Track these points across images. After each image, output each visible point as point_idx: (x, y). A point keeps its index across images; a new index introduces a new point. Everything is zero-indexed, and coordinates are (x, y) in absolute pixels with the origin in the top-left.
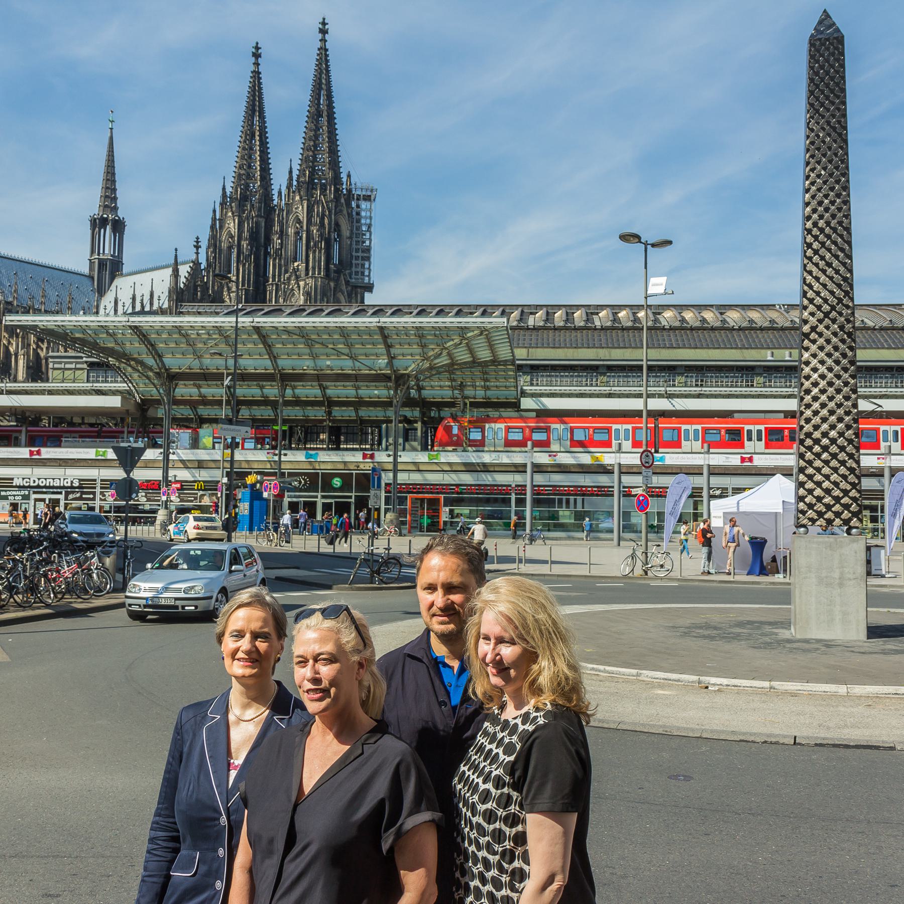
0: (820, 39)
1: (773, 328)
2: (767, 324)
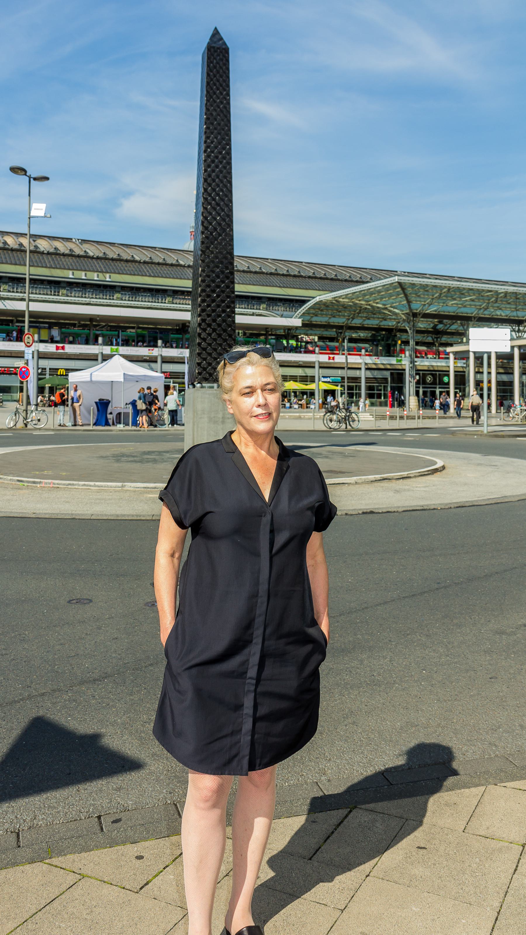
0: (214, 47)
1: (71, 255)
2: (67, 252)
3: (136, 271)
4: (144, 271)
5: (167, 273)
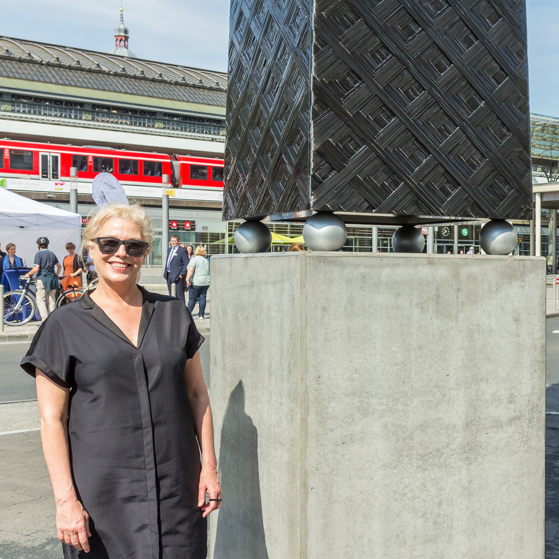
3: (36, 75)
4: (47, 76)
5: (84, 82)
